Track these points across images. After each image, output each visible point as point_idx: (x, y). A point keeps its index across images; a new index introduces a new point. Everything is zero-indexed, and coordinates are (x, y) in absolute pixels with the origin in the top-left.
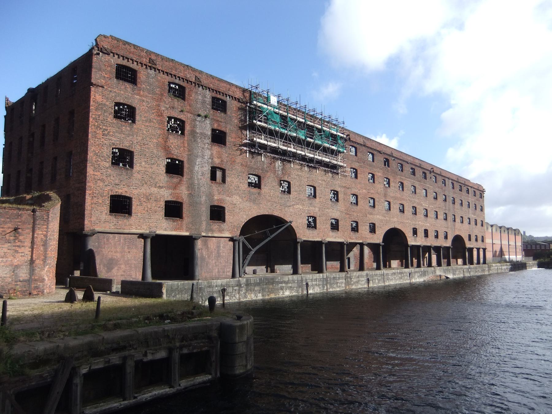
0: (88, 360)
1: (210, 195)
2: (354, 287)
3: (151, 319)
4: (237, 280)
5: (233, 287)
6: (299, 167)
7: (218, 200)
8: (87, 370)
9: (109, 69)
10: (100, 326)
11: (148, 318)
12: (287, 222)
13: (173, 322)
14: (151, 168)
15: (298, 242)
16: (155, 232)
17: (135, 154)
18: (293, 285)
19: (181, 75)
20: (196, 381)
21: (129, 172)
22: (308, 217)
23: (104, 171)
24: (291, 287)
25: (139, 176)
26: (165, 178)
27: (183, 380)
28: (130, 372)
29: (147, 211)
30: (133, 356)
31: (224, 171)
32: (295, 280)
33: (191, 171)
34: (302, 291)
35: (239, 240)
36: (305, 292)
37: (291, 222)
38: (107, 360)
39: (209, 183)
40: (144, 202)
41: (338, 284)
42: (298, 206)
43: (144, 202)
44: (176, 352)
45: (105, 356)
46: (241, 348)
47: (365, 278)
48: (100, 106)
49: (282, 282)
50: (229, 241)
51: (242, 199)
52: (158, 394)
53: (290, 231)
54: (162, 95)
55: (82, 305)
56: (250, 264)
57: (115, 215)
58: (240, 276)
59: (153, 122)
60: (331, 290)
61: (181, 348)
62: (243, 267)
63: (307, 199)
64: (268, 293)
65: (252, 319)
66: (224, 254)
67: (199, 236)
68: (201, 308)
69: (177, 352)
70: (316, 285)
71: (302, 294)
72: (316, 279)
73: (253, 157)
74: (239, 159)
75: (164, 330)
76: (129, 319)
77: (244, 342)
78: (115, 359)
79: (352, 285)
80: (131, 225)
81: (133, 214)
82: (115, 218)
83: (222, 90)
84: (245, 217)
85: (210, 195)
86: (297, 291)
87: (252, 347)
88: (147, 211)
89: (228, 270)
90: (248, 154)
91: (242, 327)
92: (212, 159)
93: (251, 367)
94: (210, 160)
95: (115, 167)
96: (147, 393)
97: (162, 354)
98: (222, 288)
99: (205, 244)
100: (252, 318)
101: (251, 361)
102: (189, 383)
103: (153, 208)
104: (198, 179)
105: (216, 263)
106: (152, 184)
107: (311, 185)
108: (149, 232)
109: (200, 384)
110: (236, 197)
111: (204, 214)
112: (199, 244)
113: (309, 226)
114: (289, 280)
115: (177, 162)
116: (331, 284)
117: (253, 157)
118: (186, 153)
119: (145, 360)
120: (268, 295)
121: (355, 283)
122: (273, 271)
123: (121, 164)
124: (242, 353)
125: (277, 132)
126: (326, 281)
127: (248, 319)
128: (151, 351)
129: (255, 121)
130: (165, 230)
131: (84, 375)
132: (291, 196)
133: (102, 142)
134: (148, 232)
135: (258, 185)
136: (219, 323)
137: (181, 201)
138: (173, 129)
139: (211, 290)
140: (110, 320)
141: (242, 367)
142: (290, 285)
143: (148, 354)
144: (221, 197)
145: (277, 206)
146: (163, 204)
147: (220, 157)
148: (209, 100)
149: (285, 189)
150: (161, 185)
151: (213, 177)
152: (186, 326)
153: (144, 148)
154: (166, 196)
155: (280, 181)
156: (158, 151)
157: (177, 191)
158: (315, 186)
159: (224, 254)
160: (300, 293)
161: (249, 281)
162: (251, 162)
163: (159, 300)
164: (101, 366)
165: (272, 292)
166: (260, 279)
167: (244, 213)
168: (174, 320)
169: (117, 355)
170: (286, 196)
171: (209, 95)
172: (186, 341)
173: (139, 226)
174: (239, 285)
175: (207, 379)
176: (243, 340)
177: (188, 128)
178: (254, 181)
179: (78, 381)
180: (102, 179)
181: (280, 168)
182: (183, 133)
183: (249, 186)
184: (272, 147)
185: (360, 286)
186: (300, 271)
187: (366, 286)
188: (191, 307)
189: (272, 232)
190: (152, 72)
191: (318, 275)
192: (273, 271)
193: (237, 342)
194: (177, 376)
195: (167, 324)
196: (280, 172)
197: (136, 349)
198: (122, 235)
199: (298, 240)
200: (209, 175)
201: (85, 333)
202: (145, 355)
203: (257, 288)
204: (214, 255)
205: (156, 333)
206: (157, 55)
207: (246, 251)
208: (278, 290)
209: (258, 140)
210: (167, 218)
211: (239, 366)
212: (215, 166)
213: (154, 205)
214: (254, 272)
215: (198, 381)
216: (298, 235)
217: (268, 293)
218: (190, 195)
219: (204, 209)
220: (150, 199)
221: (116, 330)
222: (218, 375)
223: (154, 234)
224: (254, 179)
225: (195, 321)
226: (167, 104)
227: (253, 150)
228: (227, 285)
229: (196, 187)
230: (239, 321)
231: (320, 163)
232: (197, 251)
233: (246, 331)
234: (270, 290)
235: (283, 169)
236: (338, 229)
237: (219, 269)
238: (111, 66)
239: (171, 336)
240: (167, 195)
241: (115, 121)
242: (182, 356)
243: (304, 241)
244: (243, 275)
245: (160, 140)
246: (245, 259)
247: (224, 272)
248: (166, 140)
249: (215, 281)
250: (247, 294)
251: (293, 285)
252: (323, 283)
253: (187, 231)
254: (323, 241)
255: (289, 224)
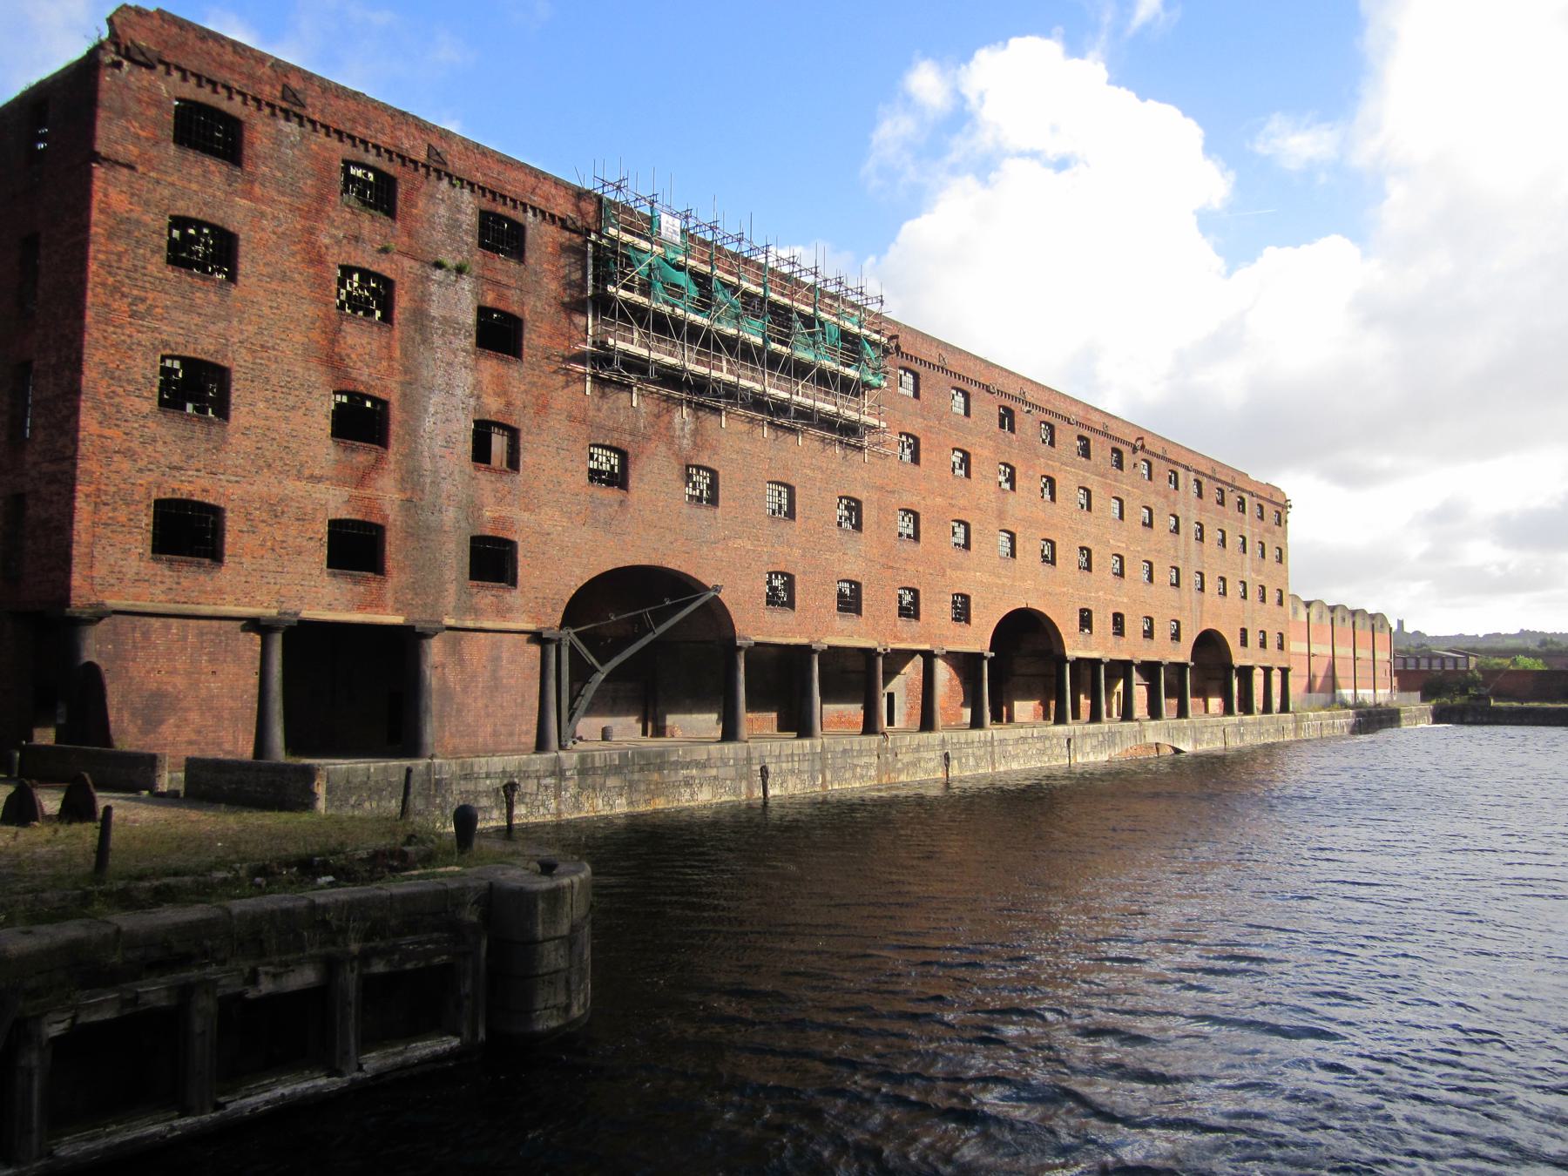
0: (68, 997)
1: (472, 508)
2: (903, 778)
3: (273, 874)
4: (551, 759)
5: (538, 778)
6: (745, 427)
7: (495, 520)
8: (62, 1026)
9: (152, 112)
10: (107, 895)
11: (263, 871)
12: (705, 588)
13: (342, 883)
14: (287, 418)
15: (740, 648)
16: (296, 614)
17: (235, 376)
18: (723, 772)
19: (384, 140)
20: (409, 1055)
21: (214, 430)
22: (770, 574)
23: (136, 425)
24: (716, 778)
25: (248, 445)
26: (332, 451)
27: (370, 1052)
28: (204, 1032)
29: (273, 550)
30: (215, 982)
31: (513, 434)
32: (729, 759)
33: (413, 433)
34: (750, 790)
35: (560, 639)
36: (759, 793)
37: (717, 588)
38: (129, 996)
39: (467, 470)
40: (263, 521)
41: (858, 770)
42: (739, 541)
43: (263, 521)
44: (348, 968)
45: (124, 986)
46: (553, 957)
47: (938, 753)
48: (122, 227)
49: (690, 763)
50: (529, 641)
51: (570, 518)
52: (293, 1094)
53: (716, 614)
54: (322, 198)
55: (56, 831)
56: (591, 711)
57: (171, 562)
58: (561, 747)
59: (293, 280)
60: (836, 787)
61: (365, 957)
62: (570, 720)
63: (767, 522)
64: (647, 797)
65: (586, 872)
66: (512, 682)
67: (437, 625)
68: (432, 841)
69: (352, 971)
70: (792, 771)
71: (748, 799)
72: (792, 755)
73: (603, 396)
74: (562, 399)
75: (313, 907)
76: (202, 875)
77: (561, 938)
78: (155, 991)
79: (900, 771)
80: (220, 591)
81: (227, 559)
82: (171, 569)
83: (511, 190)
84: (578, 572)
85: (472, 508)
86: (736, 791)
87: (587, 953)
88: (273, 550)
89: (524, 728)
90: (588, 385)
91: (555, 896)
92: (479, 398)
93: (582, 1012)
94: (472, 402)
95: (171, 413)
96: (259, 1094)
97: (304, 977)
98: (505, 782)
99: (455, 650)
100: (588, 868)
101: (582, 996)
102: (390, 1061)
103: (290, 540)
104: (434, 456)
105: (487, 706)
106: (287, 468)
107: (778, 479)
108: (279, 614)
109: (423, 1061)
110: (550, 513)
111: (452, 561)
112: (435, 650)
113: (772, 599)
114: (709, 759)
115: (368, 404)
116: (835, 771)
117: (603, 396)
118: (397, 378)
119: (252, 994)
120: (647, 802)
121: (907, 766)
122: (660, 731)
123: (190, 407)
124: (556, 972)
125: (678, 323)
126: (821, 761)
127: (576, 872)
128: (270, 969)
129: (611, 289)
130: (330, 607)
131: (55, 1041)
132: (719, 511)
133: (130, 336)
134: (274, 612)
135: (617, 480)
136: (484, 883)
137: (380, 522)
138: (355, 303)
139: (471, 786)
140: (141, 877)
141: (555, 1012)
142: (714, 772)
143: (262, 978)
144: (505, 512)
145: (676, 540)
146: (323, 530)
147: (502, 392)
148: (469, 219)
149: (701, 492)
150: (317, 472)
151: (481, 452)
152: (383, 893)
153: (262, 358)
154: (332, 505)
155: (688, 467)
156: (309, 369)
157: (368, 492)
158: (792, 483)
159: (512, 682)
160: (744, 797)
161: (589, 760)
162: (599, 410)
163: (305, 817)
164: (108, 1014)
165: (654, 792)
166: (623, 756)
167: (576, 560)
168: (344, 875)
169: (162, 980)
170: (704, 512)
171: (469, 205)
172: (382, 938)
173: (246, 594)
174: (558, 772)
175: (445, 1050)
176: (559, 934)
177: (402, 302)
178: (605, 467)
179: (33, 1059)
180: (129, 449)
181: (687, 429)
182: (387, 318)
183: (591, 479)
184: (664, 366)
185: (921, 776)
186: (744, 731)
187: (940, 775)
188: (401, 839)
189: (660, 617)
190: (291, 128)
191: (798, 742)
192: (660, 731)
193: (541, 938)
194: (352, 1040)
195: (322, 888)
196: (685, 441)
197: (223, 962)
198: (192, 623)
199: (738, 643)
200: (469, 446)
201: (60, 915)
202: (253, 979)
203: (612, 782)
204: (480, 685)
205: (287, 913)
206: (308, 77)
207: (581, 673)
208: (676, 785)
209: (621, 345)
210: (337, 571)
211: (546, 1008)
212: (487, 417)
213: (293, 532)
214: (606, 733)
215: (417, 1053)
216: (739, 627)
217: (647, 797)
218: (409, 505)
219: (452, 546)
220: (283, 512)
221: (160, 906)
222: (482, 1035)
223: (295, 619)
224: (606, 461)
225: (410, 878)
226: (337, 228)
227: (605, 375)
228: (520, 771)
229: (428, 481)
230: (545, 878)
231: (806, 415)
232: (428, 673)
233: (567, 908)
234: (652, 787)
235: (696, 432)
236: (858, 611)
237: (495, 725)
238: (158, 103)
239: (334, 923)
240: (336, 502)
241: (171, 274)
242: (370, 984)
243: (757, 644)
244: (570, 744)
245: (316, 335)
246: (578, 694)
247: (511, 734)
248: (334, 336)
249: (483, 760)
250: (583, 799)
251: (723, 772)
252: (813, 767)
253: (397, 611)
254: (814, 646)
255: (712, 594)
